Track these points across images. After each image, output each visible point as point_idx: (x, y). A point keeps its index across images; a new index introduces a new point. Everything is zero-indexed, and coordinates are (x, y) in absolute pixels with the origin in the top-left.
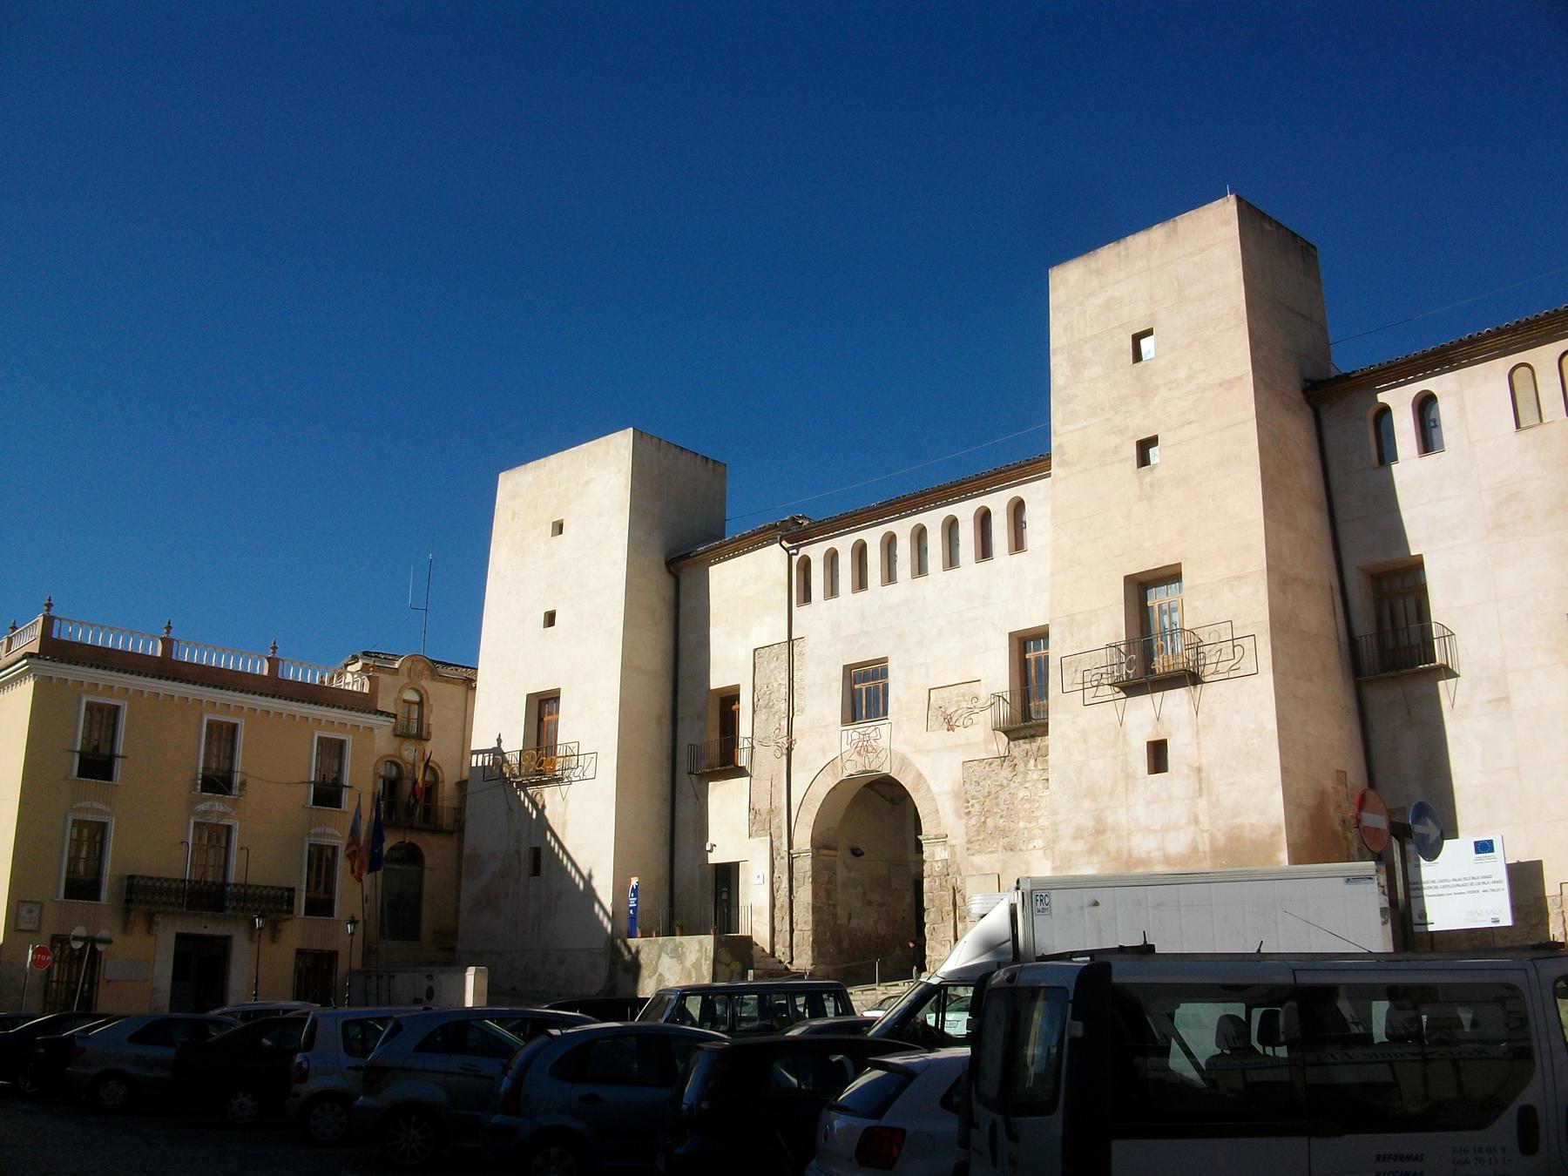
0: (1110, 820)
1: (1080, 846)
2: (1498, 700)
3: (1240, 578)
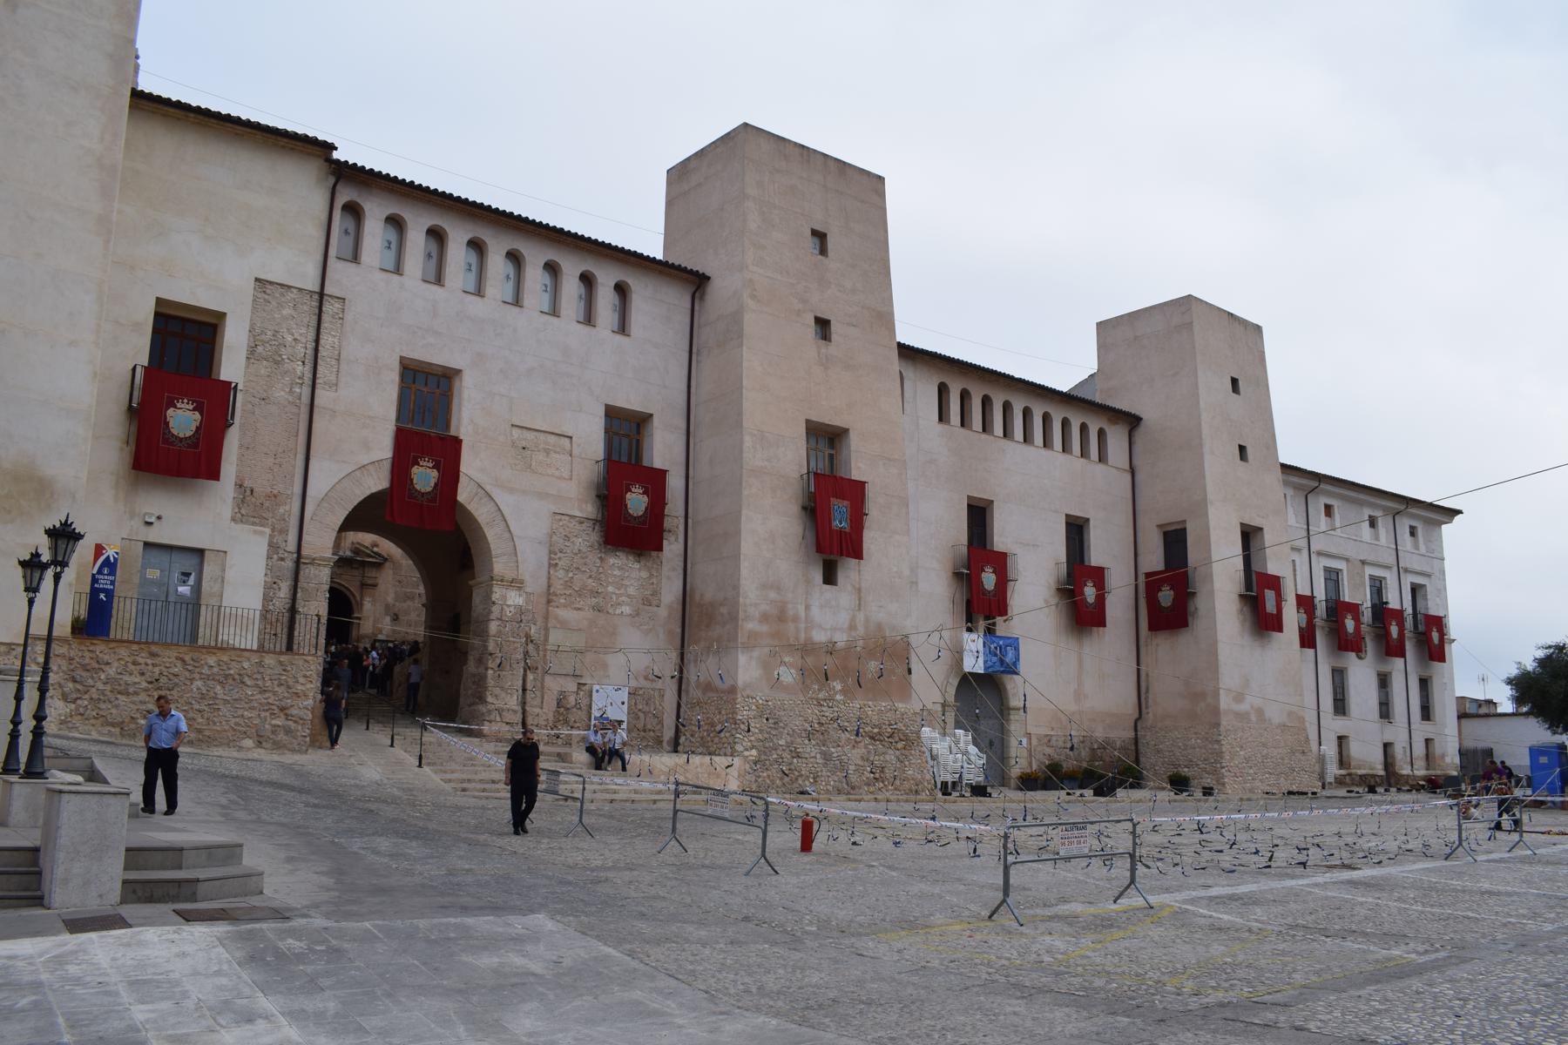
0: (791, 613)
1: (765, 628)
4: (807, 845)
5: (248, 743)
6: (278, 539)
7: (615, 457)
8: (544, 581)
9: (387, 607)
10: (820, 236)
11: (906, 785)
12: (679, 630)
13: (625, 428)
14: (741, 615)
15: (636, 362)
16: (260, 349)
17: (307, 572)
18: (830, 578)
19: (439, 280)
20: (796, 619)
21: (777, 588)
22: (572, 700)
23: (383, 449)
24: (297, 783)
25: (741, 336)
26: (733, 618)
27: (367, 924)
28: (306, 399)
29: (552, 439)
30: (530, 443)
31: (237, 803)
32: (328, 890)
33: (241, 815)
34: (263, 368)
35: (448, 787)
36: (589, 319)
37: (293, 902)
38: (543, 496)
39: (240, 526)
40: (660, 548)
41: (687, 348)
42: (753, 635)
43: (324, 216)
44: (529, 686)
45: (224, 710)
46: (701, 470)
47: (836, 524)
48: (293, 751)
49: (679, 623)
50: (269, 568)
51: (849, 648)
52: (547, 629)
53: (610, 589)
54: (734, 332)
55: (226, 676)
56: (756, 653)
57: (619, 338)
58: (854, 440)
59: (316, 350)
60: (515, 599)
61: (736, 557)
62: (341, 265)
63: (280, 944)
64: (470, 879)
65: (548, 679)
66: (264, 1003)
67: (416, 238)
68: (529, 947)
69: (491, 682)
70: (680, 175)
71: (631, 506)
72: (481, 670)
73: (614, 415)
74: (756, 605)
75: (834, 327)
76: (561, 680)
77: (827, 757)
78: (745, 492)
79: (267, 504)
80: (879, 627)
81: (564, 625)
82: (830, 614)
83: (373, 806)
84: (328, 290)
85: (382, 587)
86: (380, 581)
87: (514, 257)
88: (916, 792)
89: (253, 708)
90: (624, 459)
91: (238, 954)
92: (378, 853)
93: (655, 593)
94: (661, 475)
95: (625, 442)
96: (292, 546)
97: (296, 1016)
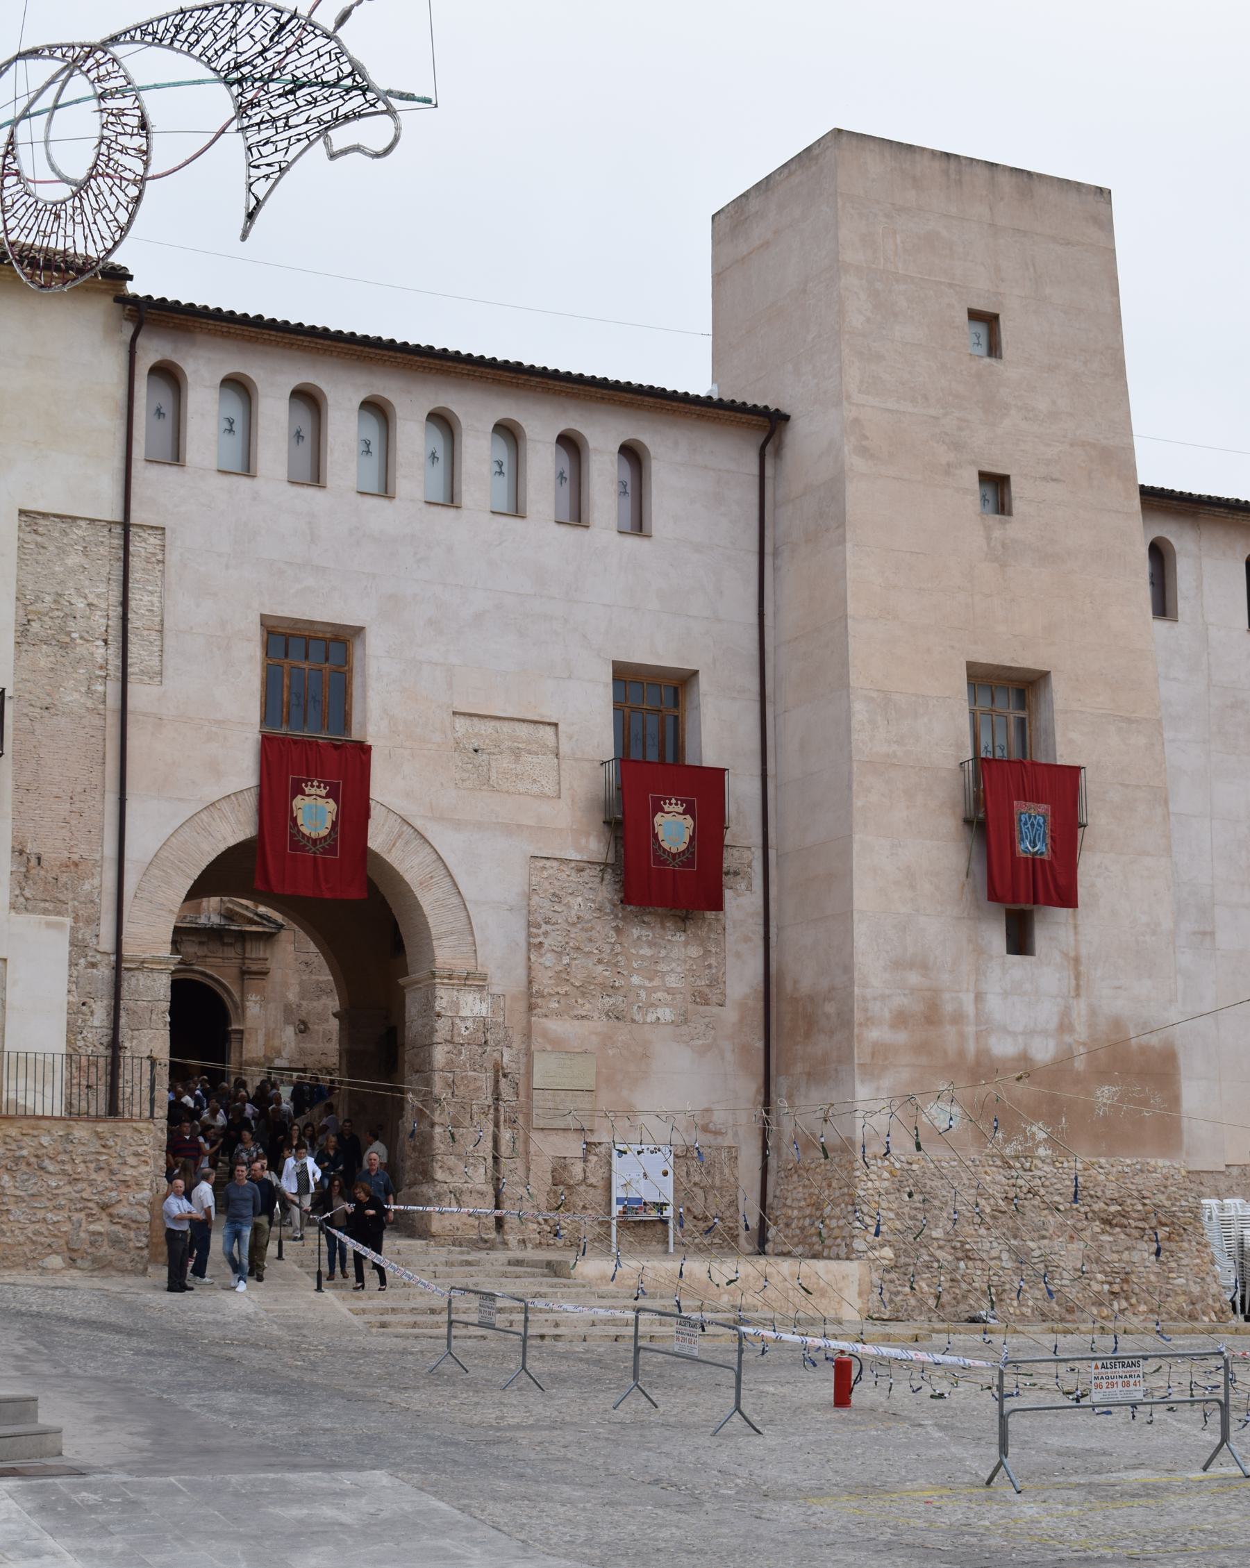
0: (949, 1008)
1: (901, 1037)
2: (1204, 933)
3: (1129, 721)
4: (842, 1397)
5: (56, 1261)
6: (85, 933)
7: (636, 754)
8: (521, 972)
9: (288, 1010)
10: (987, 321)
11: (1172, 1304)
12: (760, 1045)
13: (651, 701)
14: (858, 1016)
15: (661, 582)
16: (35, 626)
17: (134, 983)
18: (1020, 943)
19: (316, 478)
20: (958, 1018)
21: (924, 967)
22: (577, 1169)
23: (243, 772)
24: (126, 1321)
25: (842, 524)
26: (846, 1022)
27: (172, 1479)
28: (113, 701)
29: (523, 730)
30: (485, 742)
31: (37, 1352)
32: (141, 1451)
33: (44, 1368)
34: (43, 658)
35: (357, 1321)
36: (577, 516)
37: (94, 1462)
38: (511, 829)
39: (24, 917)
40: (718, 905)
41: (755, 546)
42: (882, 1053)
43: (121, 393)
44: (505, 1150)
45: (17, 1212)
46: (785, 764)
47: (1025, 847)
48: (123, 1271)
49: (760, 1032)
50: (74, 981)
51: (1060, 1069)
52: (529, 1054)
53: (636, 980)
54: (831, 518)
55: (17, 1160)
56: (887, 1082)
57: (632, 542)
58: (1060, 693)
59: (125, 619)
60: (472, 1006)
61: (847, 916)
62: (154, 472)
63: (73, 1497)
64: (325, 1439)
65: (534, 1136)
66: (50, 1543)
67: (274, 410)
68: (348, 1502)
69: (440, 1146)
70: (731, 222)
71: (667, 831)
72: (424, 1127)
73: (628, 679)
74: (883, 998)
75: (1017, 488)
76: (554, 1138)
77: (1021, 1258)
78: (858, 803)
79: (64, 878)
80: (1117, 1024)
81: (558, 1045)
82: (1021, 1005)
83: (233, 1352)
84: (135, 518)
85: (276, 974)
86: (272, 965)
87: (442, 421)
88: (1193, 1317)
89: (59, 1208)
90: (652, 756)
91: (28, 1505)
92: (215, 1410)
93: (715, 982)
94: (716, 776)
95: (652, 721)
96: (107, 944)
97: (78, 1553)
